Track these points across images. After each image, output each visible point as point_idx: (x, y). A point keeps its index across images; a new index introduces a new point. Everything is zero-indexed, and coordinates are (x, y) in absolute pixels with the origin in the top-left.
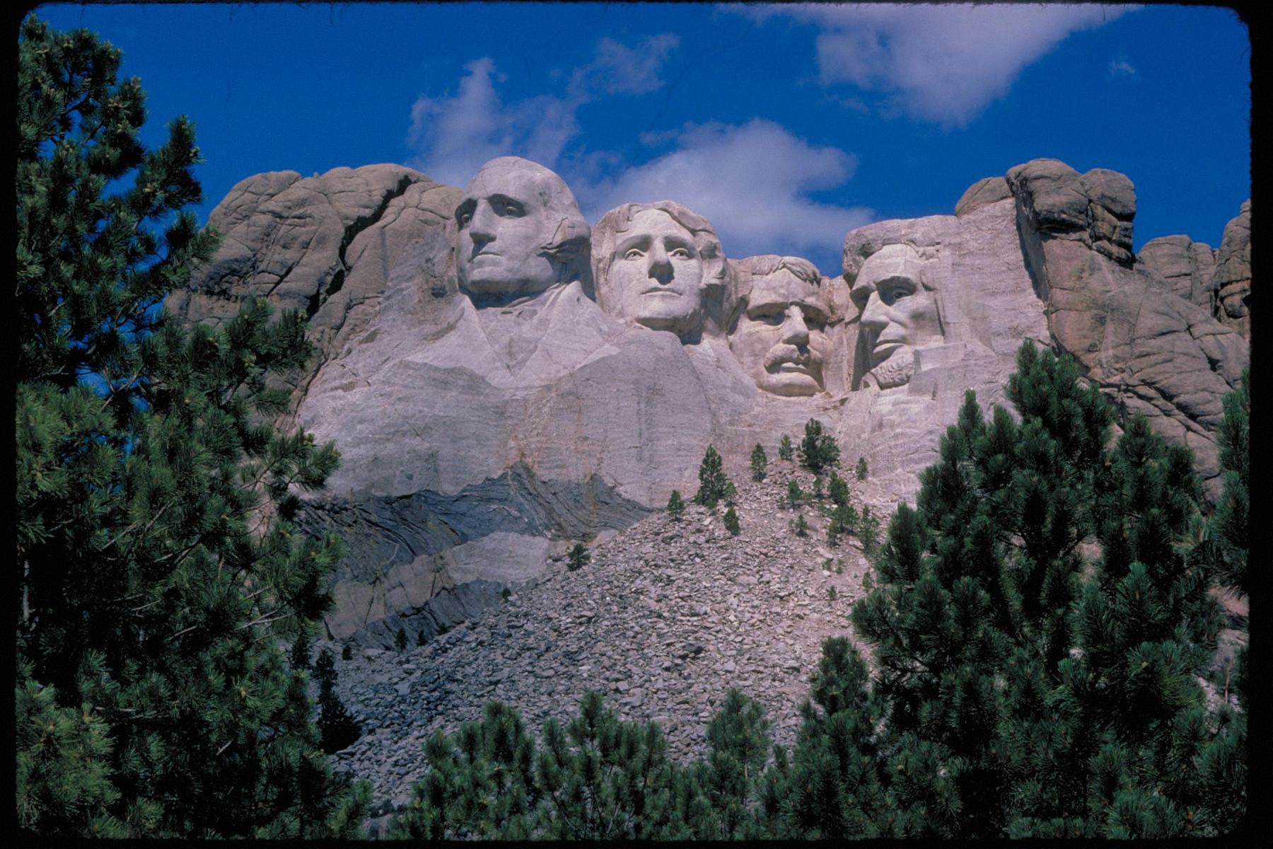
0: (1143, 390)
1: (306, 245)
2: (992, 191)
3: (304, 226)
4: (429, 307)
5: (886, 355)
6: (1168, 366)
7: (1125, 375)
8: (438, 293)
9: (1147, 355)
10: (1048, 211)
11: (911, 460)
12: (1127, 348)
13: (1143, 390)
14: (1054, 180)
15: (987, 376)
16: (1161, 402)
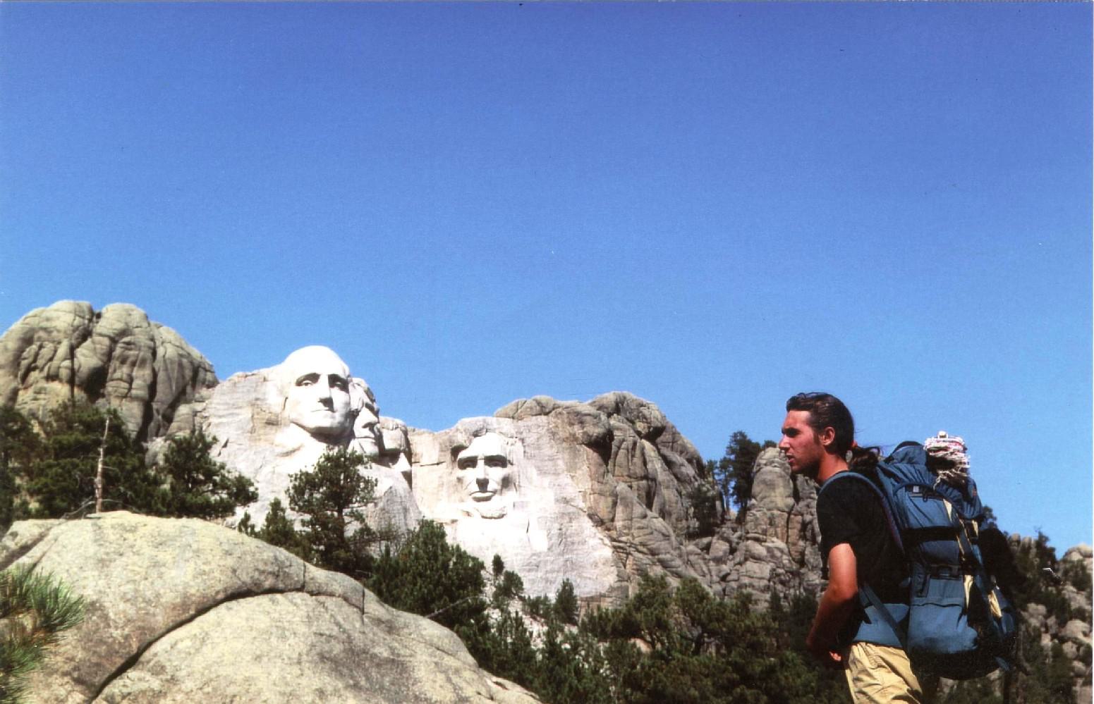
0: (641, 548)
1: (133, 364)
2: (531, 408)
3: (130, 349)
4: (262, 431)
5: (488, 499)
6: (651, 537)
7: (630, 538)
8: (272, 423)
9: (643, 528)
10: (597, 437)
11: (524, 570)
12: (629, 522)
13: (641, 548)
14: (596, 418)
15: (557, 526)
16: (650, 557)
